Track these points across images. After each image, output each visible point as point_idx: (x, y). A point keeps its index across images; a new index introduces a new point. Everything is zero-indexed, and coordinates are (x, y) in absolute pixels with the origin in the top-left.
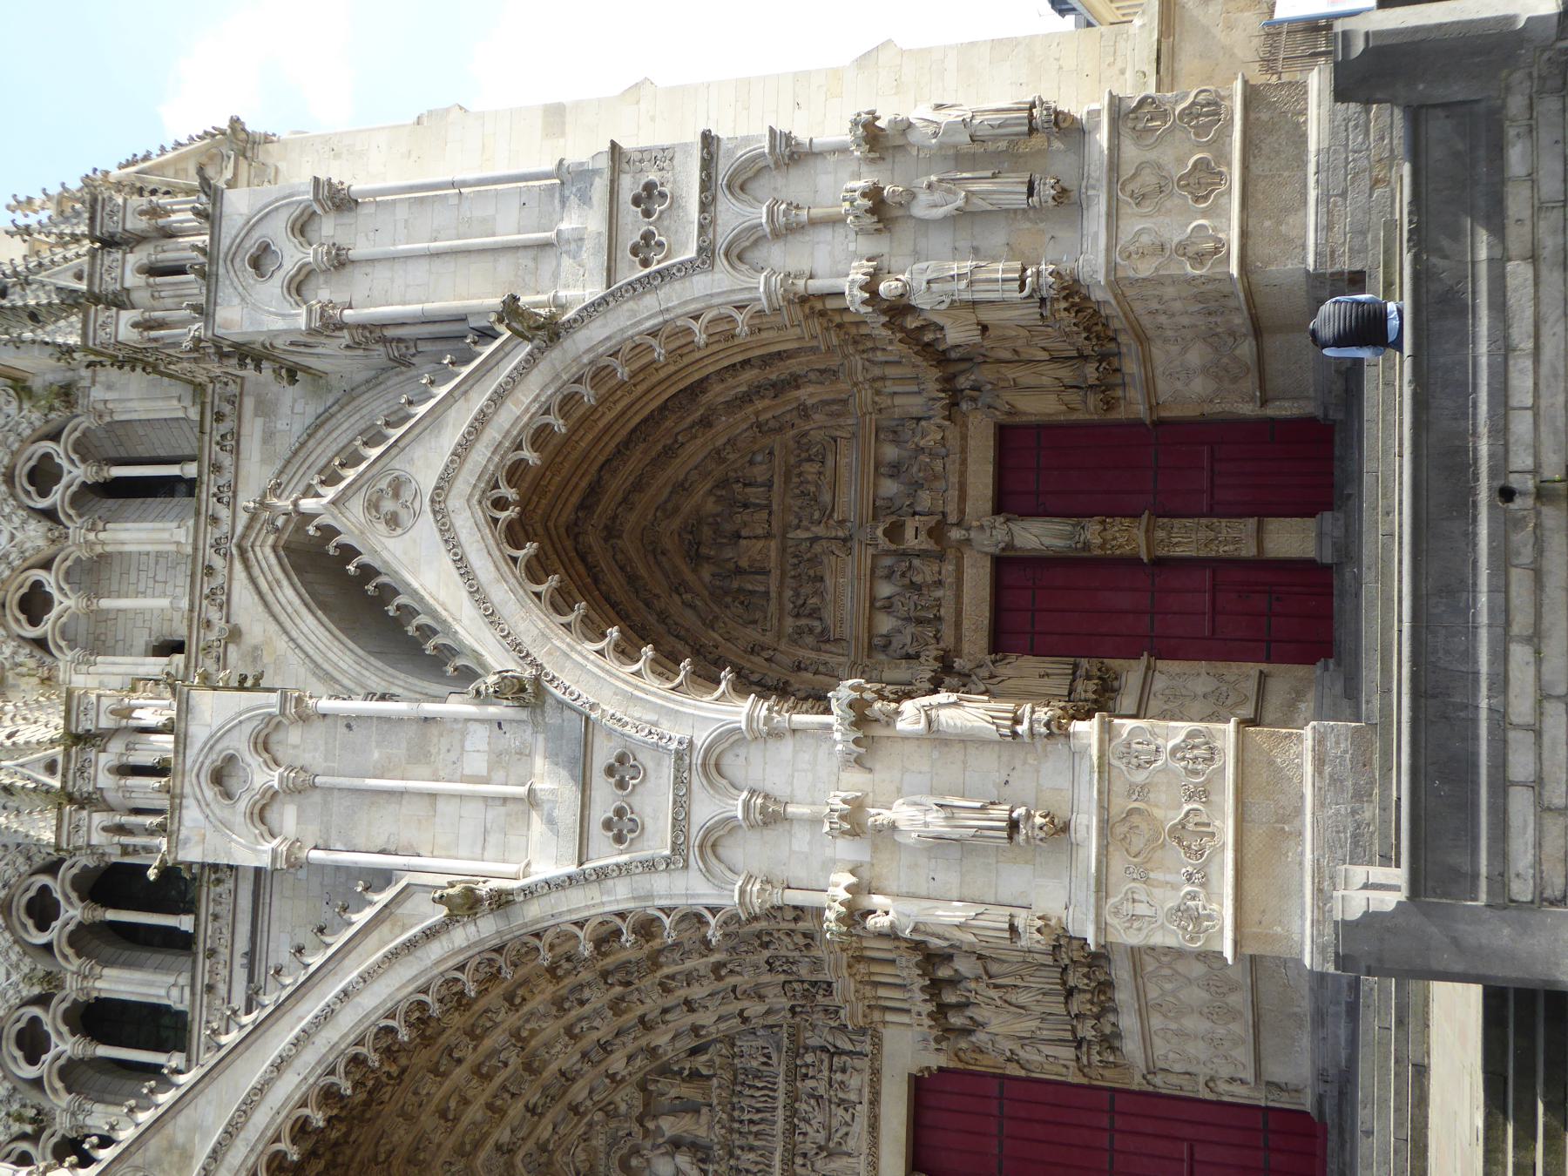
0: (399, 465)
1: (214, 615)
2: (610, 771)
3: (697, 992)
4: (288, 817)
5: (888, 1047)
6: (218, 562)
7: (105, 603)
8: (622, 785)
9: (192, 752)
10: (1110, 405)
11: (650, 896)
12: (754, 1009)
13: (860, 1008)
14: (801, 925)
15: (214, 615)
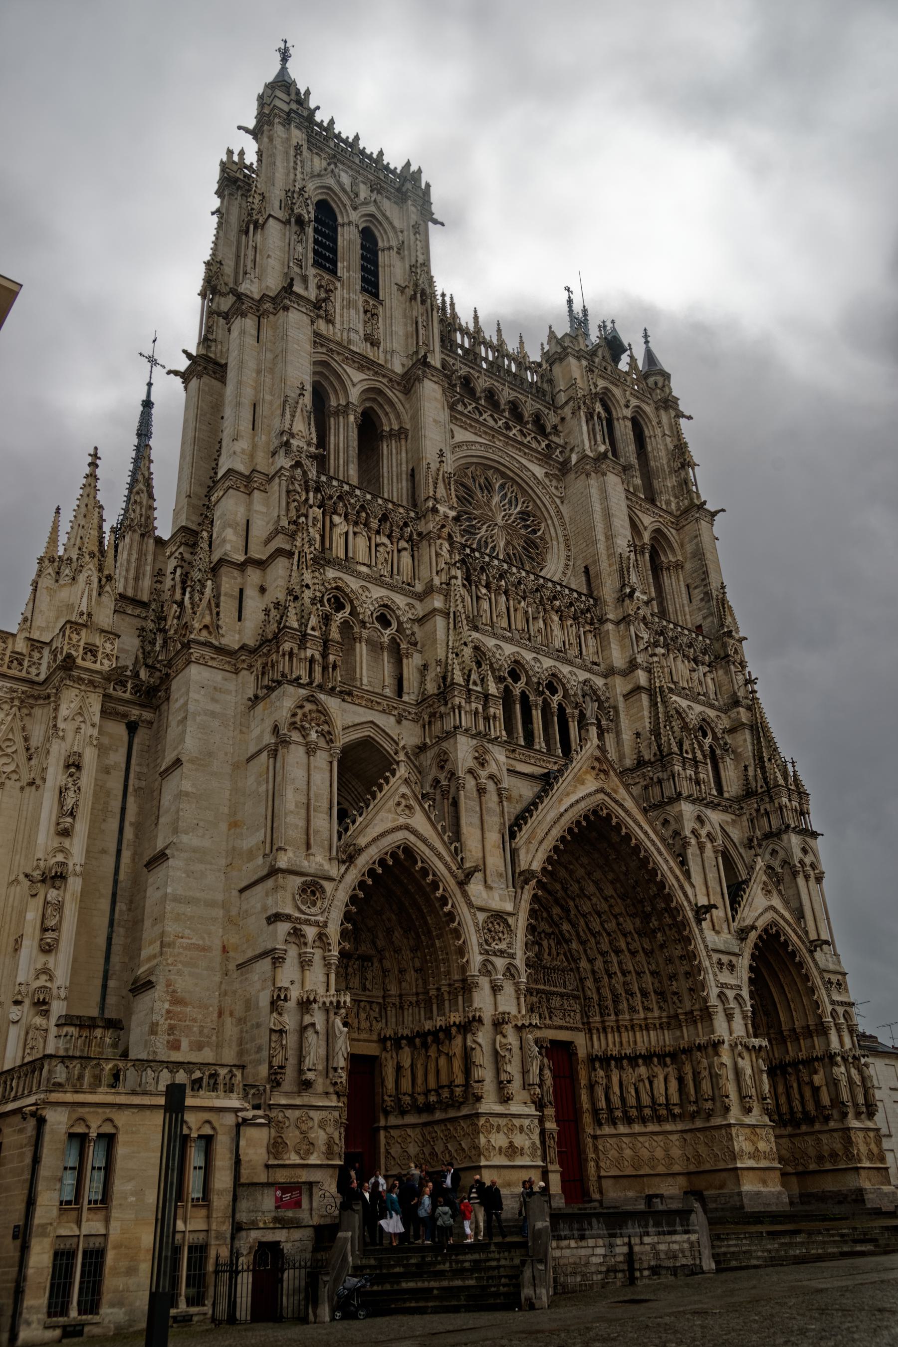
3: (599, 964)
12: (589, 983)
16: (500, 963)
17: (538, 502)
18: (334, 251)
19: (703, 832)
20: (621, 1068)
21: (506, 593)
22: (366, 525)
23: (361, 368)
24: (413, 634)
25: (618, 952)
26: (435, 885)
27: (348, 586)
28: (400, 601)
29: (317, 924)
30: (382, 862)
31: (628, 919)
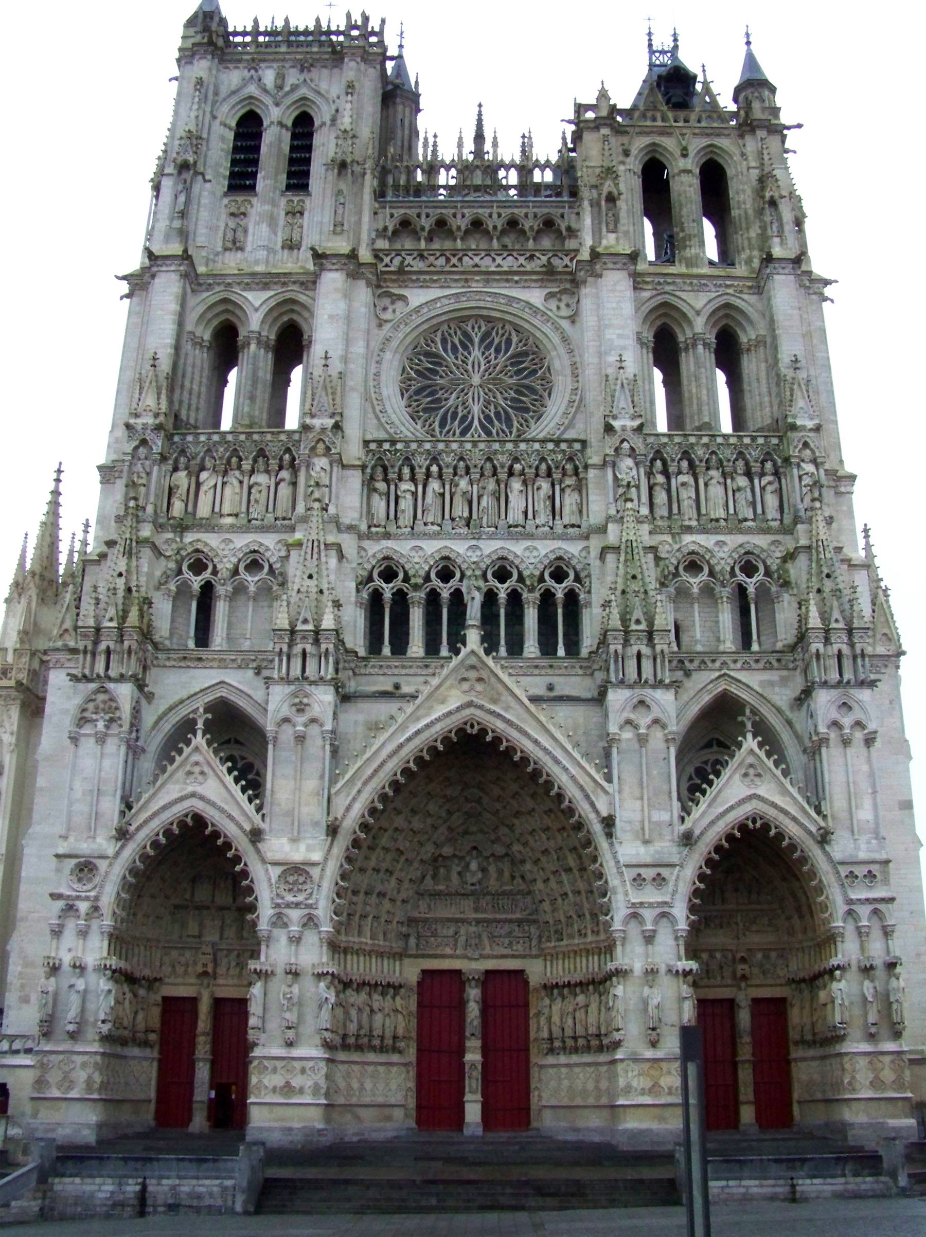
0: (768, 776)
1: (696, 663)
2: (659, 875)
3: (553, 883)
4: (627, 735)
5: (535, 961)
6: (718, 664)
7: (696, 606)
8: (654, 879)
9: (649, 692)
10: (796, 1043)
11: (616, 893)
12: (546, 906)
13: (553, 952)
14: (589, 932)
15: (696, 663)
16: (295, 915)
17: (538, 334)
18: (256, 162)
19: (644, 720)
20: (564, 998)
21: (440, 476)
22: (239, 467)
23: (266, 286)
24: (281, 574)
25: (569, 870)
26: (228, 845)
27: (206, 544)
28: (270, 542)
29: (87, 898)
30: (168, 833)
31: (571, 832)
